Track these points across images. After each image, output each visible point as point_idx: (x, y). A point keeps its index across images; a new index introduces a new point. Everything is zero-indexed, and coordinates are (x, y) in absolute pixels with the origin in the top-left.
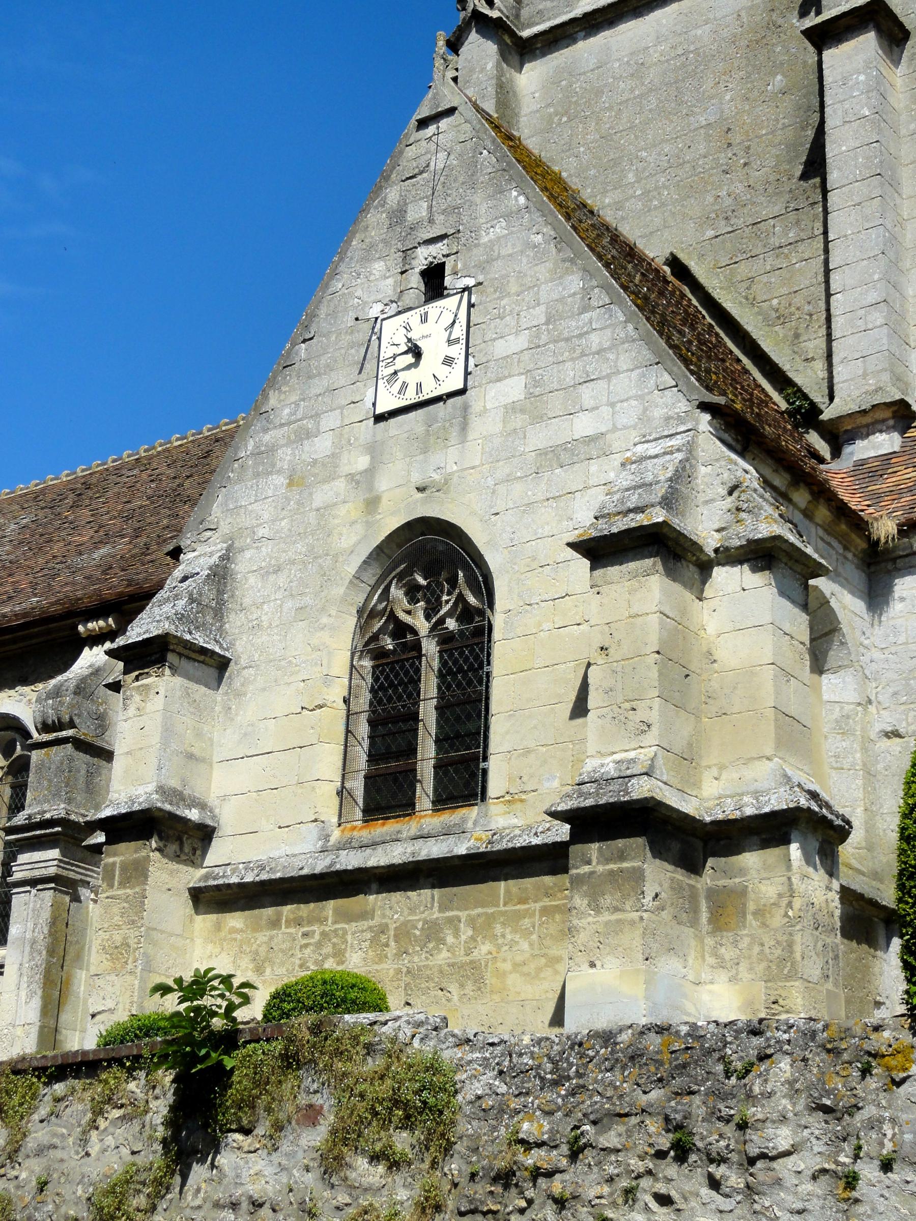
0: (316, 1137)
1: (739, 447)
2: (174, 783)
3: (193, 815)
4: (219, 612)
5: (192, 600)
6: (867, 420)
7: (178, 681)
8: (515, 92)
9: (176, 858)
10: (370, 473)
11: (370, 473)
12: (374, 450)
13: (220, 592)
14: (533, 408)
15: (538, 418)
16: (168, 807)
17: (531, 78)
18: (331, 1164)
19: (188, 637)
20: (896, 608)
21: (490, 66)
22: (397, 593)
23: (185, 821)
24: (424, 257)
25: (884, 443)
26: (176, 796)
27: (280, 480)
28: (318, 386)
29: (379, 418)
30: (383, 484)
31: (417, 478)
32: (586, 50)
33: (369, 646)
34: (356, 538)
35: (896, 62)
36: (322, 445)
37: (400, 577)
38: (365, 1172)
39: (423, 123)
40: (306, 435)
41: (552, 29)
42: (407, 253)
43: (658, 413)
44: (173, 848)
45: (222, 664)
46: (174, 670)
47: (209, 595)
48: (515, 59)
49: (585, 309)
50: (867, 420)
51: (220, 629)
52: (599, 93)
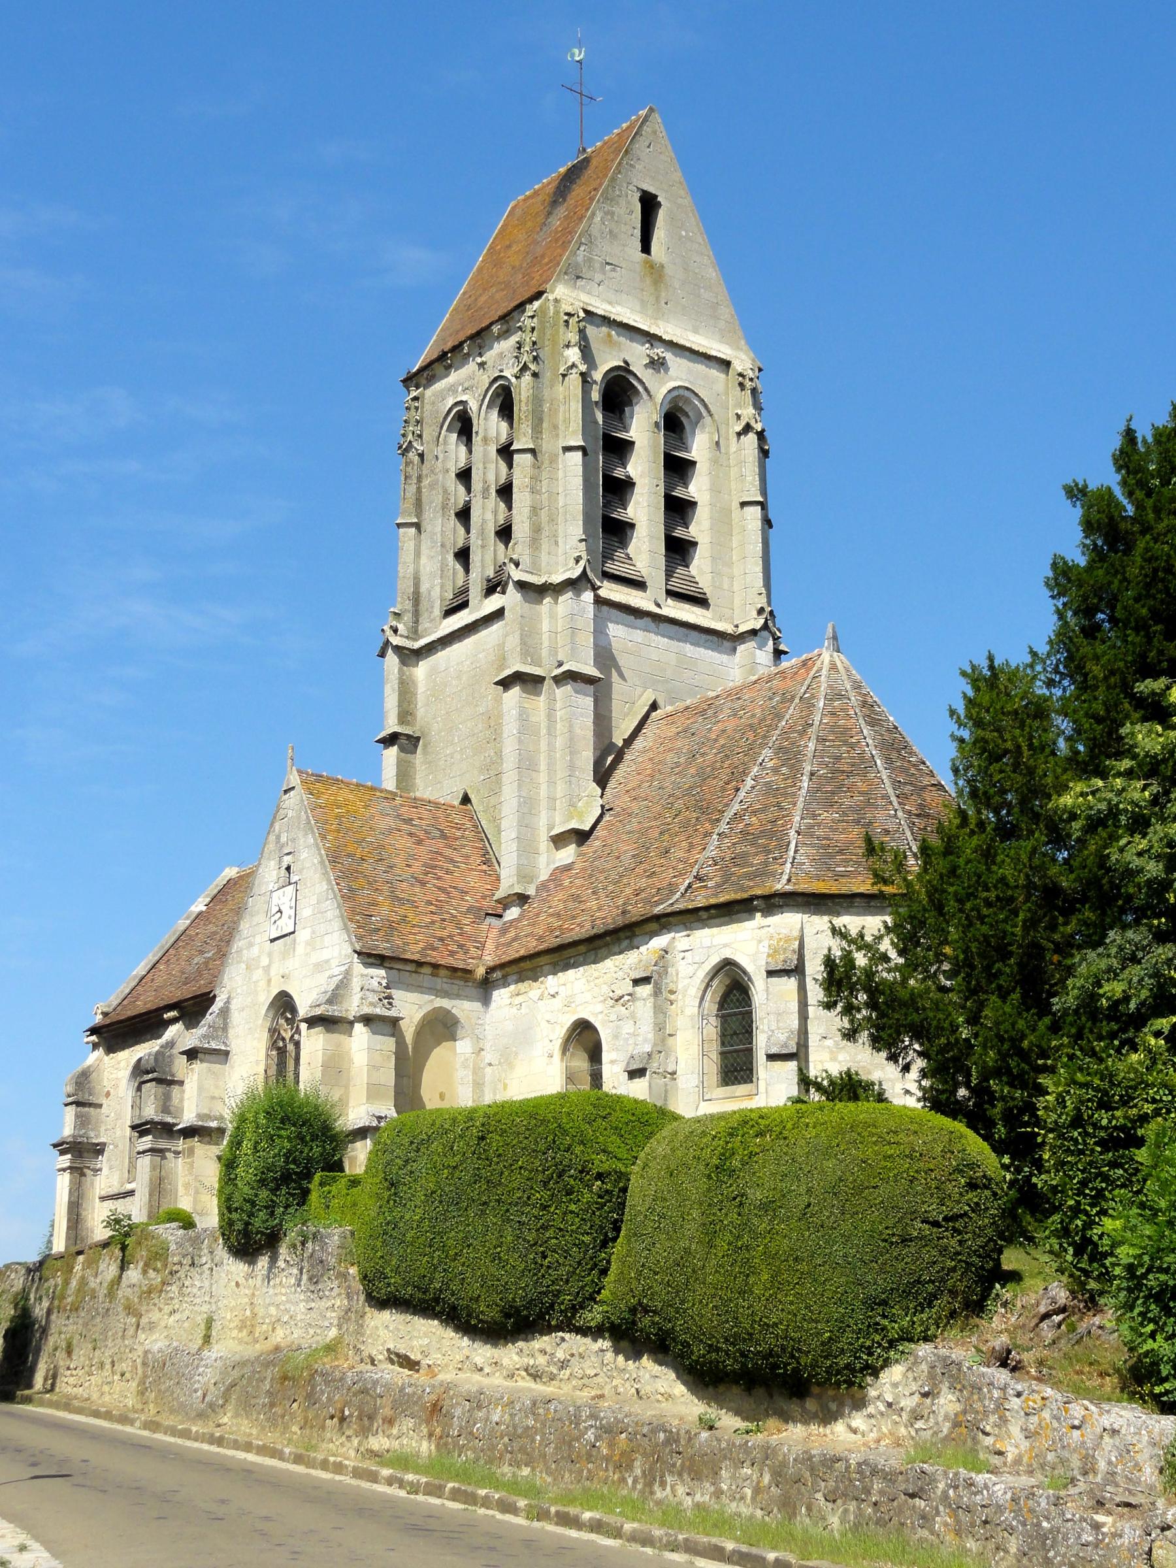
0: (141, 1264)
1: (378, 962)
2: (206, 1111)
3: (214, 1124)
4: (225, 1029)
5: (210, 1027)
6: (509, 900)
7: (205, 1065)
8: (413, 682)
9: (209, 1143)
10: (269, 966)
11: (269, 966)
12: (270, 955)
13: (225, 1019)
14: (311, 943)
15: (314, 949)
16: (200, 1123)
17: (421, 670)
18: (145, 1272)
19: (206, 1046)
20: (493, 1005)
21: (396, 671)
22: (282, 1021)
23: (211, 1128)
24: (287, 860)
25: (513, 913)
26: (208, 1117)
27: (243, 966)
28: (256, 919)
29: (272, 941)
30: (273, 972)
31: (281, 973)
32: (442, 656)
33: (273, 1045)
34: (265, 998)
35: (539, 694)
36: (255, 951)
37: (282, 1014)
38: (152, 1274)
39: (286, 792)
40: (251, 945)
41: (426, 645)
42: (280, 862)
43: (343, 952)
44: (207, 1139)
45: (227, 1053)
46: (201, 1061)
47: (220, 1022)
48: (414, 659)
49: (327, 899)
50: (509, 900)
51: (227, 1037)
52: (446, 686)
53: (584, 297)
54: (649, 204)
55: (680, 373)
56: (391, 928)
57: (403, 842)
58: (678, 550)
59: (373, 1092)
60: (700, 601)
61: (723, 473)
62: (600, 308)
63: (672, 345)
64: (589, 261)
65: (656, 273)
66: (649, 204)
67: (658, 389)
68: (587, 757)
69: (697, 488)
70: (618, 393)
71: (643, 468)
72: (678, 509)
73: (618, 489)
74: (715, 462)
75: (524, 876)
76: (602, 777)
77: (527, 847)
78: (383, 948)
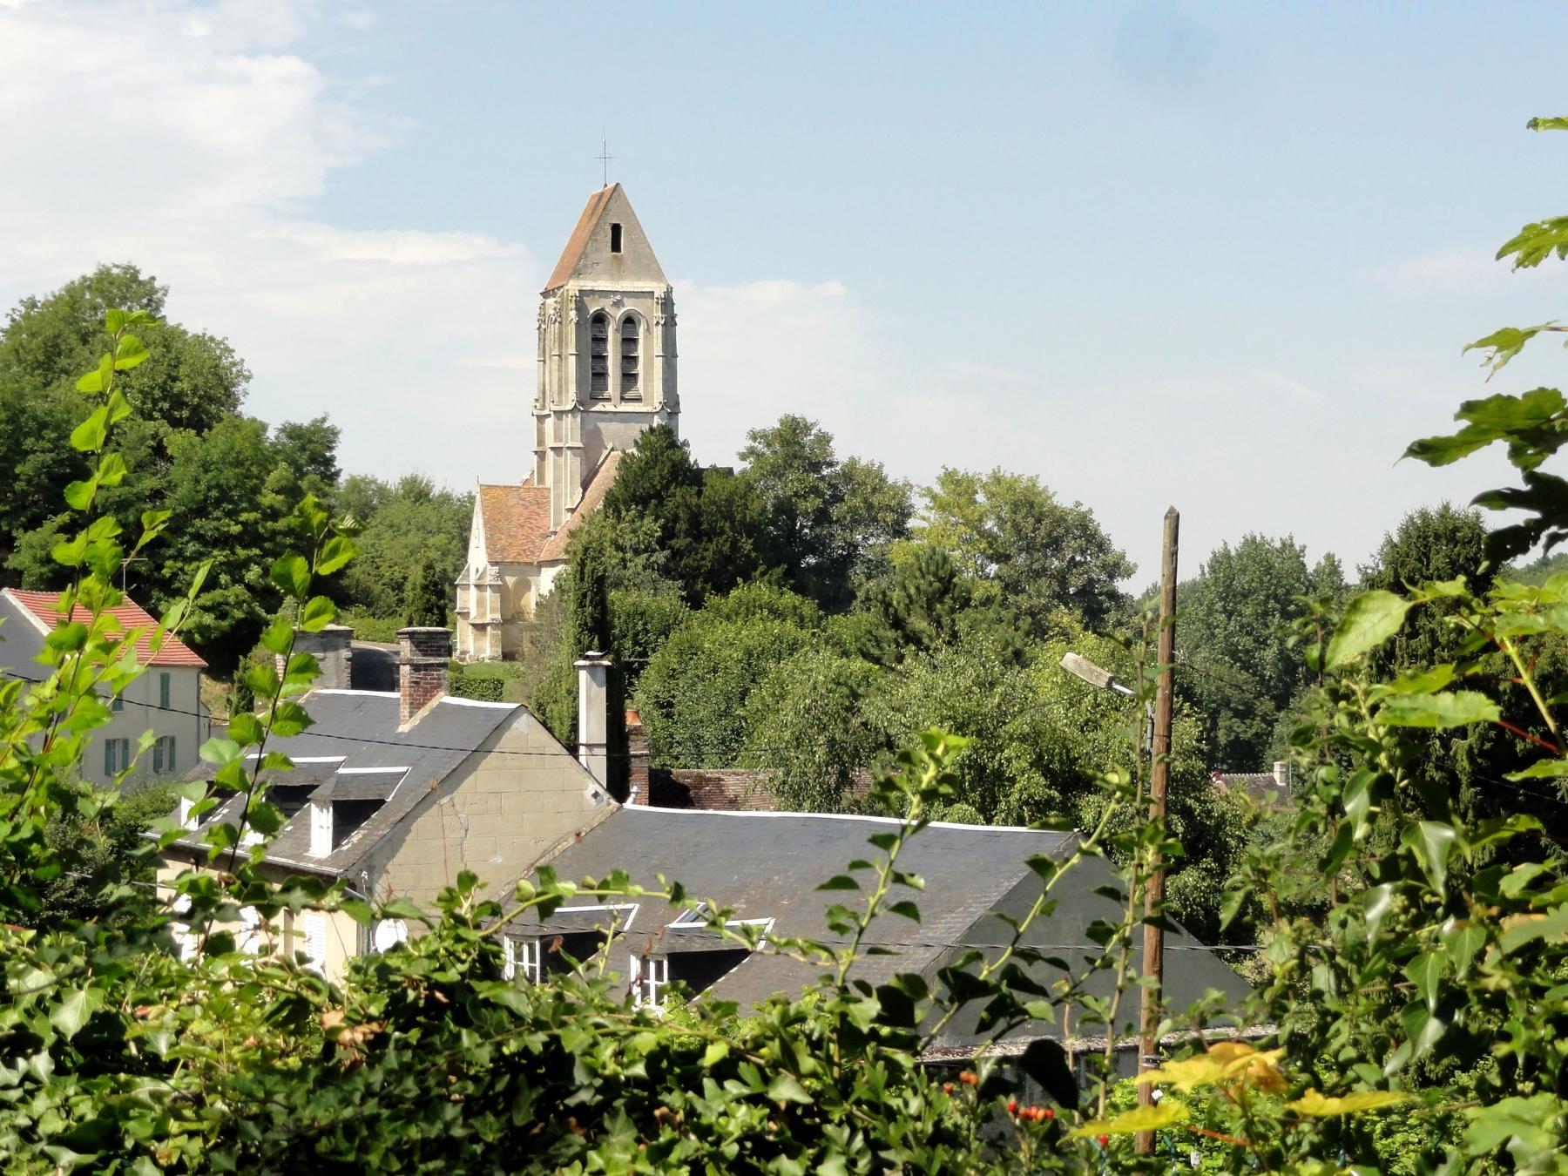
53: (582, 283)
54: (616, 229)
55: (629, 305)
56: (504, 549)
57: (520, 509)
58: (629, 378)
59: (492, 611)
60: (639, 400)
61: (649, 346)
62: (588, 285)
63: (624, 293)
64: (585, 266)
65: (619, 261)
66: (616, 229)
67: (617, 314)
68: (578, 479)
69: (640, 352)
70: (600, 319)
71: (612, 352)
72: (629, 360)
73: (600, 358)
74: (646, 338)
75: (556, 524)
76: (585, 485)
77: (558, 513)
78: (498, 558)
